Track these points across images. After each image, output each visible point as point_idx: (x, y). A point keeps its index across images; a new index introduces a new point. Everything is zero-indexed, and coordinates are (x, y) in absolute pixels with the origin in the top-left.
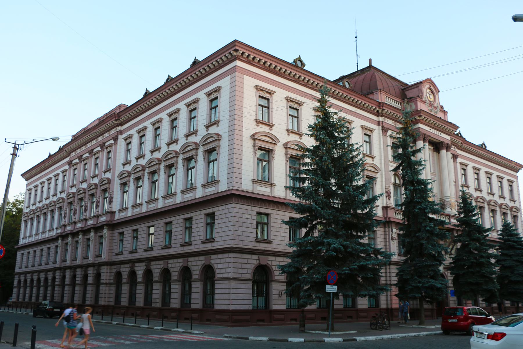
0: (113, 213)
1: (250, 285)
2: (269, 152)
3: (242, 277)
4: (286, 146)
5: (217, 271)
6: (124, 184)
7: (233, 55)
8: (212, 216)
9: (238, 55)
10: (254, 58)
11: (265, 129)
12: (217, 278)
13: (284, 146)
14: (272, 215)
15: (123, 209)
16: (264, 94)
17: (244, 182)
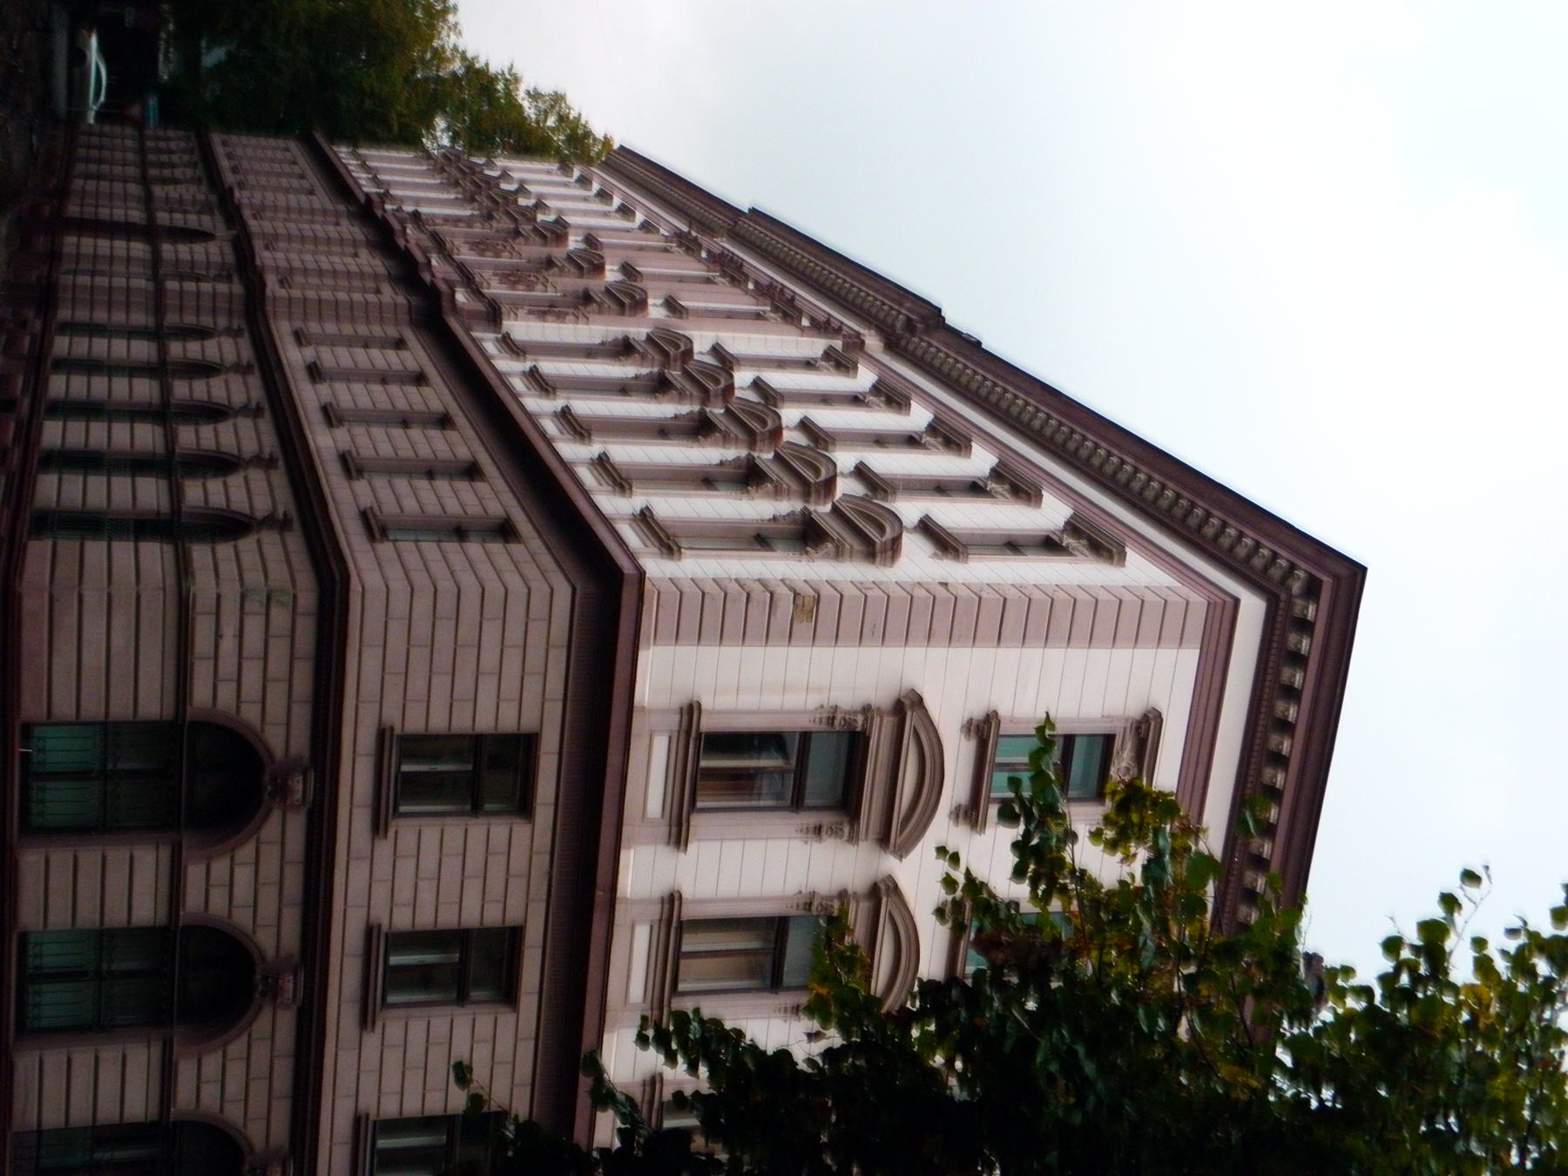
0: (493, 315)
1: (153, 703)
2: (846, 804)
3: (197, 663)
4: (882, 892)
5: (225, 550)
6: (623, 349)
7: (1290, 581)
8: (505, 531)
9: (1290, 604)
10: (1286, 727)
11: (956, 787)
12: (187, 545)
13: (883, 880)
14: (528, 828)
15: (515, 349)
16: (1124, 764)
17: (686, 653)
